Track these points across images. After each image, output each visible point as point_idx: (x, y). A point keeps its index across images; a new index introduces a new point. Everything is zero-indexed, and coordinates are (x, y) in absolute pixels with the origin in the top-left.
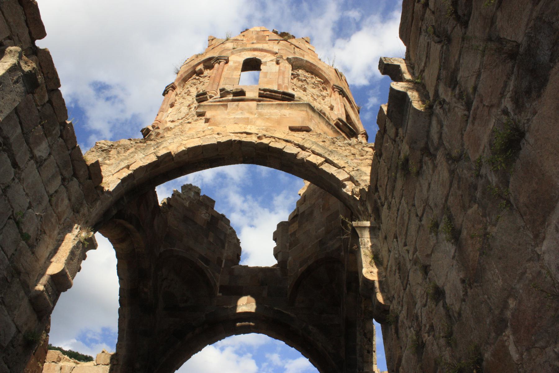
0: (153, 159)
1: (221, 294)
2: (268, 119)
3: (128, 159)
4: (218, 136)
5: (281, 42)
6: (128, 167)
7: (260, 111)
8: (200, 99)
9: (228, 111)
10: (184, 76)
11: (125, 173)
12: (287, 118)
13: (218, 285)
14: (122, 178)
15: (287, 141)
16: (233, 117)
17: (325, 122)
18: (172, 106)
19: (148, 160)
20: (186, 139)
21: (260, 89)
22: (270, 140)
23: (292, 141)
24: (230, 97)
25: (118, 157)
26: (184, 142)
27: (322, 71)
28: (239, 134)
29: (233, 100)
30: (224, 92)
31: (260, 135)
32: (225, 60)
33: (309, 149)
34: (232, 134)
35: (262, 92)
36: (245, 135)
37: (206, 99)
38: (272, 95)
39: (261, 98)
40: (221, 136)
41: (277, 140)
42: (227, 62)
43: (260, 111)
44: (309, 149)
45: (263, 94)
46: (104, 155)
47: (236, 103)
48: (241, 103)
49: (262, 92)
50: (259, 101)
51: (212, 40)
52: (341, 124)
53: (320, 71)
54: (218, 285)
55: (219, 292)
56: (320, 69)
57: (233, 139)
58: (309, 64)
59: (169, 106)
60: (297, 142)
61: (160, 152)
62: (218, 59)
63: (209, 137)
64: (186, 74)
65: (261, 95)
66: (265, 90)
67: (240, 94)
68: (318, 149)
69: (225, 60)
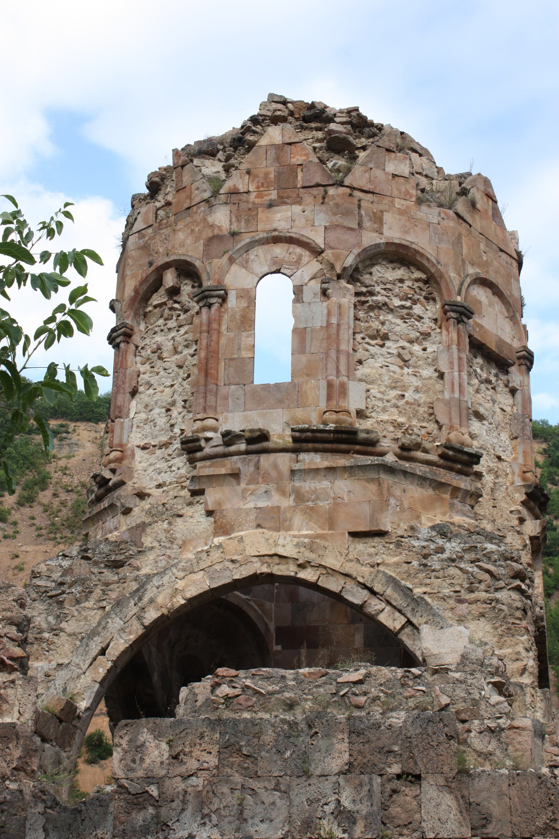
0: (141, 631)
1: (279, 648)
2: (312, 509)
3: (99, 634)
4: (234, 566)
5: (332, 191)
6: (103, 652)
7: (297, 484)
8: (190, 448)
9: (243, 485)
10: (141, 292)
11: (102, 668)
12: (346, 505)
13: (272, 626)
14: (99, 680)
15: (347, 575)
16: (251, 505)
17: (416, 481)
18: (134, 393)
19: (130, 633)
20: (182, 574)
21: (293, 430)
22: (318, 573)
23: (354, 576)
24: (243, 446)
25: (80, 613)
26: (180, 584)
27: (422, 255)
28: (266, 558)
29: (247, 452)
30: (229, 438)
31: (301, 561)
32: (219, 296)
33: (382, 595)
34: (255, 560)
35: (297, 434)
36: (276, 559)
37: (201, 449)
38: (317, 437)
39: (298, 445)
40: (237, 565)
41: (330, 571)
42: (224, 299)
43: (297, 484)
44: (382, 595)
45: (300, 437)
46: (56, 609)
47: (254, 457)
48: (264, 458)
49: (297, 434)
50: (295, 451)
51: (183, 167)
52: (451, 453)
53: (418, 258)
54: (272, 626)
55: (276, 645)
56: (417, 252)
57: (258, 572)
58: (393, 248)
59: (128, 396)
60: (361, 580)
61: (146, 615)
62: (206, 297)
63: (218, 567)
64: (145, 287)
65: (295, 440)
66: (301, 431)
67: (258, 440)
68: (396, 595)
69: (219, 296)
